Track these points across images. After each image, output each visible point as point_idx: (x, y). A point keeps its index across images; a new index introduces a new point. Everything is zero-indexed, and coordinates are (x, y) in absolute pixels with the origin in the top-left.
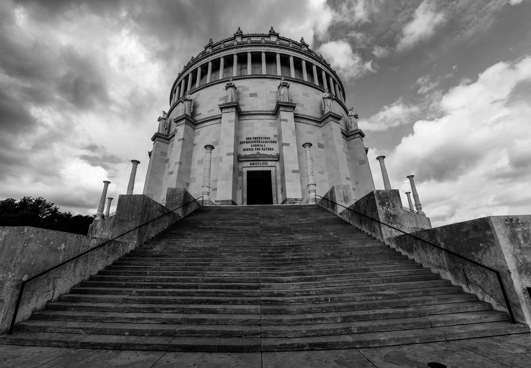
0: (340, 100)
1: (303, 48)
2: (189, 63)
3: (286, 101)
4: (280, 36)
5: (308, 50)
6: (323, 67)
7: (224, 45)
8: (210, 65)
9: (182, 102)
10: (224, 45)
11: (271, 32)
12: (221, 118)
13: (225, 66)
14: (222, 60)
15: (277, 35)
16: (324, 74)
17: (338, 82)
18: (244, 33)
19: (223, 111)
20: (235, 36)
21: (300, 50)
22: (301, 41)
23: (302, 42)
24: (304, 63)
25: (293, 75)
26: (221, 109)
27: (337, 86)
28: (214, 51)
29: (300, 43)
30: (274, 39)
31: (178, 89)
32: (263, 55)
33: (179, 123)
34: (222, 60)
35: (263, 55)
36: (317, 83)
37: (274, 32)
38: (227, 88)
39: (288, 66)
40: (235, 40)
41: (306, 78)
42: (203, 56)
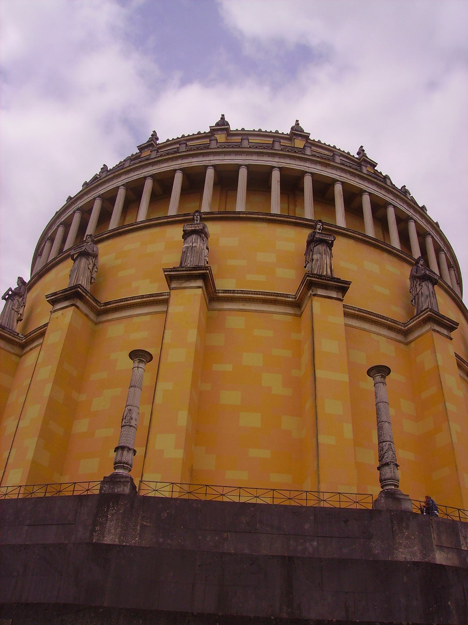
0: (449, 286)
1: (364, 168)
2: (95, 178)
3: (325, 273)
4: (311, 138)
5: (375, 173)
6: (410, 212)
7: (187, 146)
8: (149, 185)
9: (73, 259)
10: (187, 146)
11: (296, 130)
12: (166, 302)
13: (184, 192)
14: (178, 179)
15: (306, 137)
16: (412, 227)
17: (445, 249)
18: (233, 127)
19: (173, 285)
20: (213, 131)
21: (357, 170)
22: (358, 154)
23: (361, 155)
24: (366, 199)
25: (341, 220)
26: (170, 279)
27: (443, 256)
28: (161, 156)
29: (357, 156)
30: (299, 143)
31: (61, 231)
32: (276, 176)
33: (58, 306)
34: (178, 179)
35: (276, 176)
36: (395, 242)
37: (302, 131)
38: (186, 235)
39: (331, 202)
40: (213, 138)
41: (370, 230)
42: (133, 164)
